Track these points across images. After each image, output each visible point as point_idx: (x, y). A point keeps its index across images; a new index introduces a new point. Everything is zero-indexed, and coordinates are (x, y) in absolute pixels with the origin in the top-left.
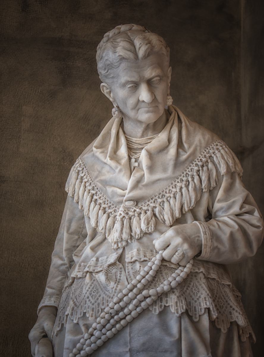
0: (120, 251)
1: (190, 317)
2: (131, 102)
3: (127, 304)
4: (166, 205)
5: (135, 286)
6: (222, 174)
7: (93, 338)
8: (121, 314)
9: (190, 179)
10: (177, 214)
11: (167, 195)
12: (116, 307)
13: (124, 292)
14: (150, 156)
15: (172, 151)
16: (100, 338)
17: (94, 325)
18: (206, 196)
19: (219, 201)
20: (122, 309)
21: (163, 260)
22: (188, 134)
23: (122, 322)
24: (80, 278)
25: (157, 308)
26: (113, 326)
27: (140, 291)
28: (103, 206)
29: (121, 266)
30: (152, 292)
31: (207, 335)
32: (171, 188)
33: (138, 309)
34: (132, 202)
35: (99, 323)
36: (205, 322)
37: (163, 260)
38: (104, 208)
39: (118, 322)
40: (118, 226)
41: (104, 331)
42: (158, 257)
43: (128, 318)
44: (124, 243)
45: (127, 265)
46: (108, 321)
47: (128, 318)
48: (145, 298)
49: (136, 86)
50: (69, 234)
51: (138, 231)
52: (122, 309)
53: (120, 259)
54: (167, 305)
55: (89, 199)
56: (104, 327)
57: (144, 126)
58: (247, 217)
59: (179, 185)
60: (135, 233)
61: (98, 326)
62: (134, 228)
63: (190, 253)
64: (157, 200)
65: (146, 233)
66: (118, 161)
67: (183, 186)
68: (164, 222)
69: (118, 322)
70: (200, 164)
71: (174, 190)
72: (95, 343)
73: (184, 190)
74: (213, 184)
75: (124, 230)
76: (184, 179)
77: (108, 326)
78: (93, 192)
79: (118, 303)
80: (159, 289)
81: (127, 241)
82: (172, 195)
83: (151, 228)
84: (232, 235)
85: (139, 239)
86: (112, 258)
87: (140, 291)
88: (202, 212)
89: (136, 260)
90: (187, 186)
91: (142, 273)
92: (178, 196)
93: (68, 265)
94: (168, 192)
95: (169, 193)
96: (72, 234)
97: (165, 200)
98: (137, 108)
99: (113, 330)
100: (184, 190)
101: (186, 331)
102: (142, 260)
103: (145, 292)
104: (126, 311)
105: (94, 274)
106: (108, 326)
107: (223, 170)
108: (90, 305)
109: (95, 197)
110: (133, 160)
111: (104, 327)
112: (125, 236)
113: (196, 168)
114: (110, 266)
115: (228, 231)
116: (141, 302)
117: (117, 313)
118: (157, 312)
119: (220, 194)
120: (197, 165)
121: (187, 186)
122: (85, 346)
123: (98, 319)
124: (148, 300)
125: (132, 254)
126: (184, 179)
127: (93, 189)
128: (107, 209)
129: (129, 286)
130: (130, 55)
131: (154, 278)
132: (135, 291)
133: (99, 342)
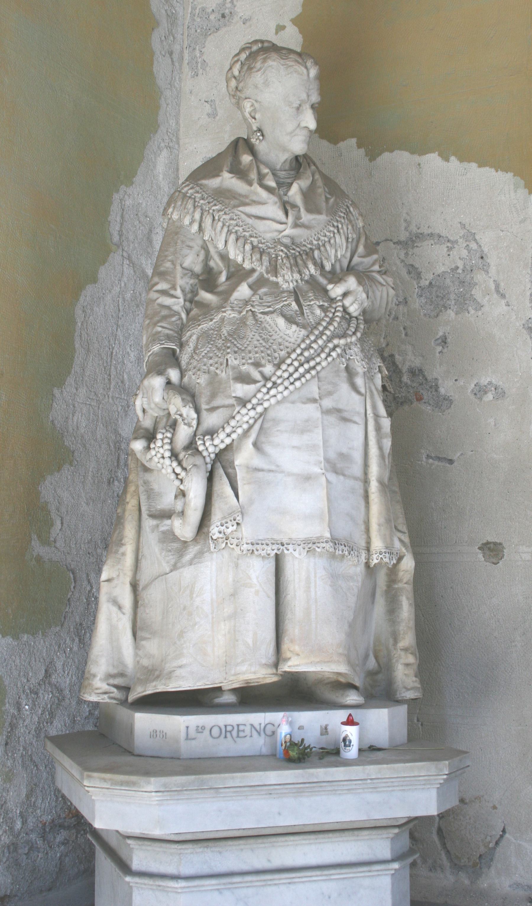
6: (358, 227)
7: (281, 388)
8: (312, 363)
9: (340, 226)
10: (333, 261)
12: (306, 354)
13: (312, 338)
16: (286, 388)
23: (313, 372)
24: (234, 317)
25: (344, 360)
26: (303, 375)
27: (330, 340)
30: (342, 342)
32: (325, 231)
35: (286, 370)
39: (308, 371)
41: (292, 380)
44: (295, 283)
45: (304, 308)
46: (296, 370)
47: (319, 368)
48: (335, 347)
50: (183, 268)
51: (308, 273)
54: (351, 358)
55: (225, 229)
56: (291, 375)
59: (332, 229)
60: (305, 274)
61: (286, 375)
64: (312, 241)
67: (336, 231)
69: (308, 371)
71: (328, 234)
72: (282, 393)
73: (337, 236)
77: (296, 375)
81: (297, 281)
82: (326, 239)
85: (307, 282)
89: (315, 303)
91: (328, 319)
93: (183, 303)
94: (322, 235)
95: (323, 236)
97: (321, 244)
98: (294, 134)
99: (303, 380)
102: (321, 303)
103: (336, 341)
106: (296, 375)
118: (345, 365)
120: (341, 212)
122: (267, 397)
123: (284, 367)
124: (339, 350)
126: (335, 224)
127: (232, 219)
130: (305, 71)
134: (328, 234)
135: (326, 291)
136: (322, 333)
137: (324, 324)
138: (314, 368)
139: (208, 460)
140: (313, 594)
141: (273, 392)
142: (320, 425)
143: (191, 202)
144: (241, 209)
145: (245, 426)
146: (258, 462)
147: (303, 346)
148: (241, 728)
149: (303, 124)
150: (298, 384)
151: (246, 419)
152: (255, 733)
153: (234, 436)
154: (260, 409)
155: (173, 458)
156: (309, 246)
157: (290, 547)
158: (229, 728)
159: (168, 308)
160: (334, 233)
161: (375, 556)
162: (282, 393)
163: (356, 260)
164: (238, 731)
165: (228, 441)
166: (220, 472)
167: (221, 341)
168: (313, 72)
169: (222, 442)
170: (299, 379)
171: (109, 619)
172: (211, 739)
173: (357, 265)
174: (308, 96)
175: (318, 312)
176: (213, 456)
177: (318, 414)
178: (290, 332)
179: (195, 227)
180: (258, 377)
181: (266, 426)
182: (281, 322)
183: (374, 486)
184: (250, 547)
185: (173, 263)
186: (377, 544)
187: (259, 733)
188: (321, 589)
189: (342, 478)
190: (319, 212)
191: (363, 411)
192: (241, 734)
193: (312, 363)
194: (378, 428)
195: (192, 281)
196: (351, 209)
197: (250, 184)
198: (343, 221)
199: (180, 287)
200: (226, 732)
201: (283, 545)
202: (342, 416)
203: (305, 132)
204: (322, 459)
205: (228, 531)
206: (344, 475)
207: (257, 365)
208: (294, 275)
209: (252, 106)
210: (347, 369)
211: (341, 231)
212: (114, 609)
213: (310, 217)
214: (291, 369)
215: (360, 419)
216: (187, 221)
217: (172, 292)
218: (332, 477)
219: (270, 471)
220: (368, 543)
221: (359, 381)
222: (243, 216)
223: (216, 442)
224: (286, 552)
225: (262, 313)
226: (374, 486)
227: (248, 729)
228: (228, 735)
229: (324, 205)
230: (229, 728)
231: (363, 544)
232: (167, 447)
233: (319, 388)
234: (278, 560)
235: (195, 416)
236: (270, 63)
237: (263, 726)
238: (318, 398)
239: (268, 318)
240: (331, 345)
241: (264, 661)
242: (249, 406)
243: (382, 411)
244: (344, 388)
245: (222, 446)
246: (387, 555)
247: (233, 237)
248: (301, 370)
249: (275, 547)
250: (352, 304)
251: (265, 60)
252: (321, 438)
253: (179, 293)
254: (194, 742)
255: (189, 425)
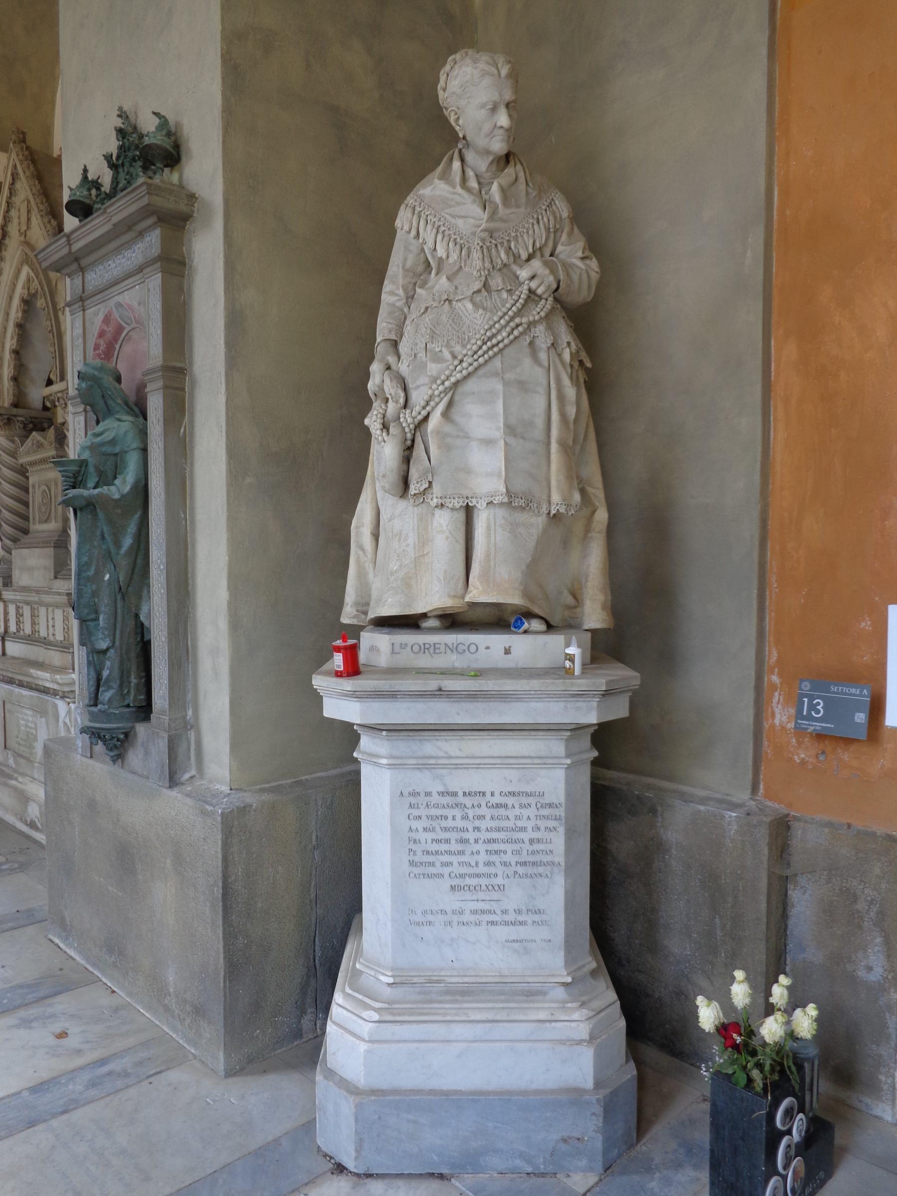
0: (483, 279)
1: (555, 349)
2: (487, 127)
3: (499, 331)
4: (520, 240)
5: (505, 314)
7: (465, 365)
8: (494, 341)
9: (540, 217)
10: (531, 250)
11: (521, 230)
12: (488, 334)
13: (496, 319)
14: (502, 190)
15: (522, 186)
16: (471, 364)
17: (464, 352)
18: (552, 235)
19: (562, 245)
20: (494, 336)
21: (530, 290)
22: (531, 174)
23: (496, 349)
27: (512, 319)
28: (453, 237)
29: (486, 294)
30: (524, 320)
31: (569, 370)
33: (512, 337)
34: (487, 233)
36: (567, 356)
37: (530, 290)
38: (455, 239)
39: (489, 349)
40: (476, 255)
41: (475, 357)
42: (526, 287)
43: (501, 345)
46: (480, 348)
47: (501, 345)
48: (518, 326)
49: (494, 110)
52: (494, 336)
53: (486, 285)
55: (434, 231)
56: (475, 353)
57: (491, 158)
58: (588, 262)
59: (531, 221)
62: (494, 258)
63: (555, 286)
65: (505, 265)
66: (469, 190)
68: (519, 257)
70: (547, 204)
71: (527, 226)
73: (536, 227)
74: (558, 226)
75: (486, 259)
76: (535, 216)
77: (480, 353)
78: (441, 223)
79: (490, 328)
80: (531, 319)
83: (512, 259)
84: (580, 275)
85: (500, 270)
86: (477, 285)
87: (512, 319)
88: (547, 252)
90: (538, 223)
91: (512, 302)
92: (531, 232)
96: (407, 270)
99: (486, 356)
100: (536, 227)
101: (554, 362)
103: (517, 320)
104: (499, 338)
105: (454, 303)
106: (480, 353)
107: (565, 214)
108: (454, 332)
109: (442, 228)
110: (483, 192)
111: (475, 353)
112: (488, 265)
113: (544, 207)
114: (474, 293)
115: (578, 271)
116: (513, 330)
117: (490, 339)
119: (564, 237)
121: (538, 223)
122: (454, 373)
123: (468, 347)
124: (520, 329)
125: (497, 281)
126: (535, 216)
128: (458, 240)
129: (500, 314)
130: (495, 72)
131: (523, 306)
132: (507, 317)
133: (471, 369)
134: (527, 226)
135: (517, 277)
136: (505, 314)
137: (508, 305)
138: (497, 344)
139: (407, 430)
140: (492, 539)
141: (458, 368)
142: (501, 396)
143: (409, 210)
144: (447, 211)
145: (437, 399)
146: (448, 428)
147: (486, 327)
148: (437, 646)
149: (499, 124)
150: (481, 360)
151: (437, 393)
152: (448, 651)
153: (428, 408)
154: (447, 384)
155: (384, 430)
156: (507, 238)
157: (474, 500)
158: (427, 646)
159: (393, 305)
160: (533, 224)
161: (553, 508)
162: (467, 369)
163: (560, 248)
164: (435, 649)
165: (424, 413)
166: (418, 439)
167: (424, 330)
168: (504, 72)
169: (420, 413)
170: (483, 355)
171: (358, 561)
172: (412, 655)
173: (560, 253)
174: (501, 95)
175: (505, 295)
176: (412, 426)
177: (499, 387)
178: (478, 316)
179: (414, 232)
180: (447, 355)
181: (457, 398)
182: (470, 306)
183: (554, 447)
184: (440, 501)
185: (398, 266)
186: (556, 498)
187: (452, 651)
188: (501, 536)
189: (521, 441)
190: (518, 206)
191: (545, 382)
192: (437, 651)
193: (494, 341)
194: (561, 398)
195: (414, 281)
196: (557, 202)
197: (454, 187)
198: (544, 212)
199: (403, 286)
200: (424, 648)
201: (467, 498)
202: (523, 386)
203: (501, 131)
204: (502, 425)
205: (422, 489)
206: (524, 438)
207: (448, 346)
208: (486, 265)
209: (456, 114)
210: (531, 344)
211: (541, 222)
212: (361, 553)
213: (508, 211)
214: (475, 348)
215: (542, 390)
216: (406, 228)
217: (396, 292)
218: (512, 440)
219: (457, 437)
220: (549, 496)
221: (543, 356)
222: (448, 217)
223: (414, 414)
224: (470, 504)
225: (457, 301)
226: (554, 447)
227: (442, 647)
228: (426, 651)
229: (523, 200)
230: (427, 646)
231: (545, 497)
232: (382, 421)
233: (502, 363)
234: (469, 511)
235: (402, 394)
236: (464, 69)
237: (455, 645)
238: (500, 371)
239: (460, 304)
240: (512, 324)
241: (452, 594)
242: (439, 382)
243: (566, 381)
244: (527, 362)
245: (420, 417)
246: (564, 506)
247: (440, 237)
248: (485, 348)
249: (461, 500)
250: (539, 286)
251: (460, 66)
252: (501, 407)
253: (401, 292)
254: (398, 656)
255: (397, 402)
